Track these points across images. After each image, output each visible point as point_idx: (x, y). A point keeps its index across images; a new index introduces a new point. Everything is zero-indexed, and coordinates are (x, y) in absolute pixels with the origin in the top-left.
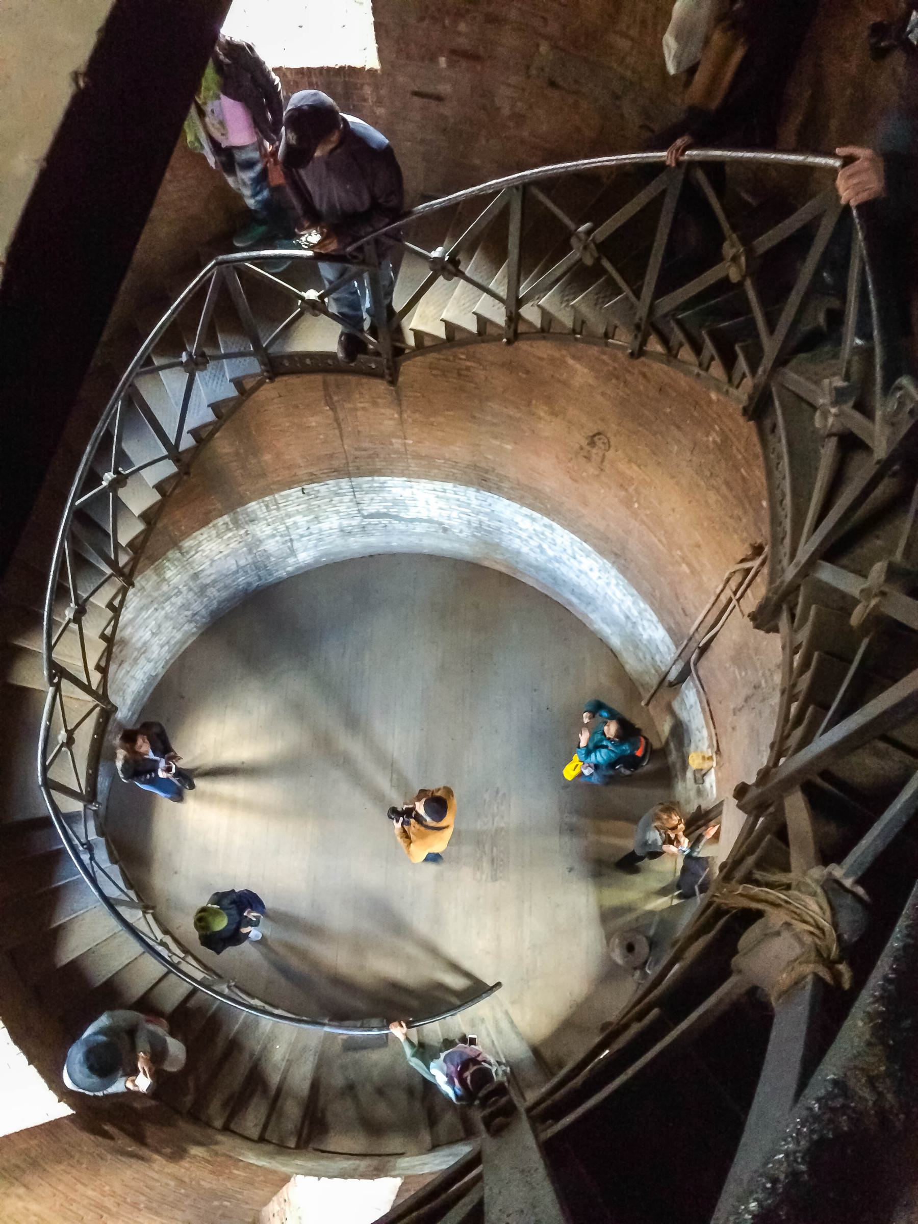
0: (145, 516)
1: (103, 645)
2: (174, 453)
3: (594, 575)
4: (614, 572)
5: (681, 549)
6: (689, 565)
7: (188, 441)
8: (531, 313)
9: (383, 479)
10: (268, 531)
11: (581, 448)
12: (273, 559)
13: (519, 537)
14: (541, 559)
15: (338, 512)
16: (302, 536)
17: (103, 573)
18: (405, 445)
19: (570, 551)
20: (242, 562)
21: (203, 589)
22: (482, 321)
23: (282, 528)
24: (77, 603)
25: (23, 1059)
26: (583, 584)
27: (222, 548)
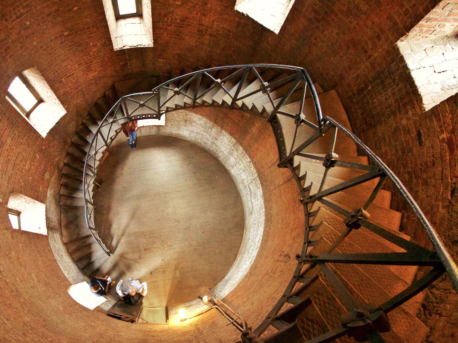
0: (214, 101)
2: (235, 99)
7: (239, 103)
11: (284, 252)
14: (248, 247)
15: (247, 177)
19: (251, 256)
20: (225, 152)
21: (213, 143)
23: (238, 161)
27: (226, 144)
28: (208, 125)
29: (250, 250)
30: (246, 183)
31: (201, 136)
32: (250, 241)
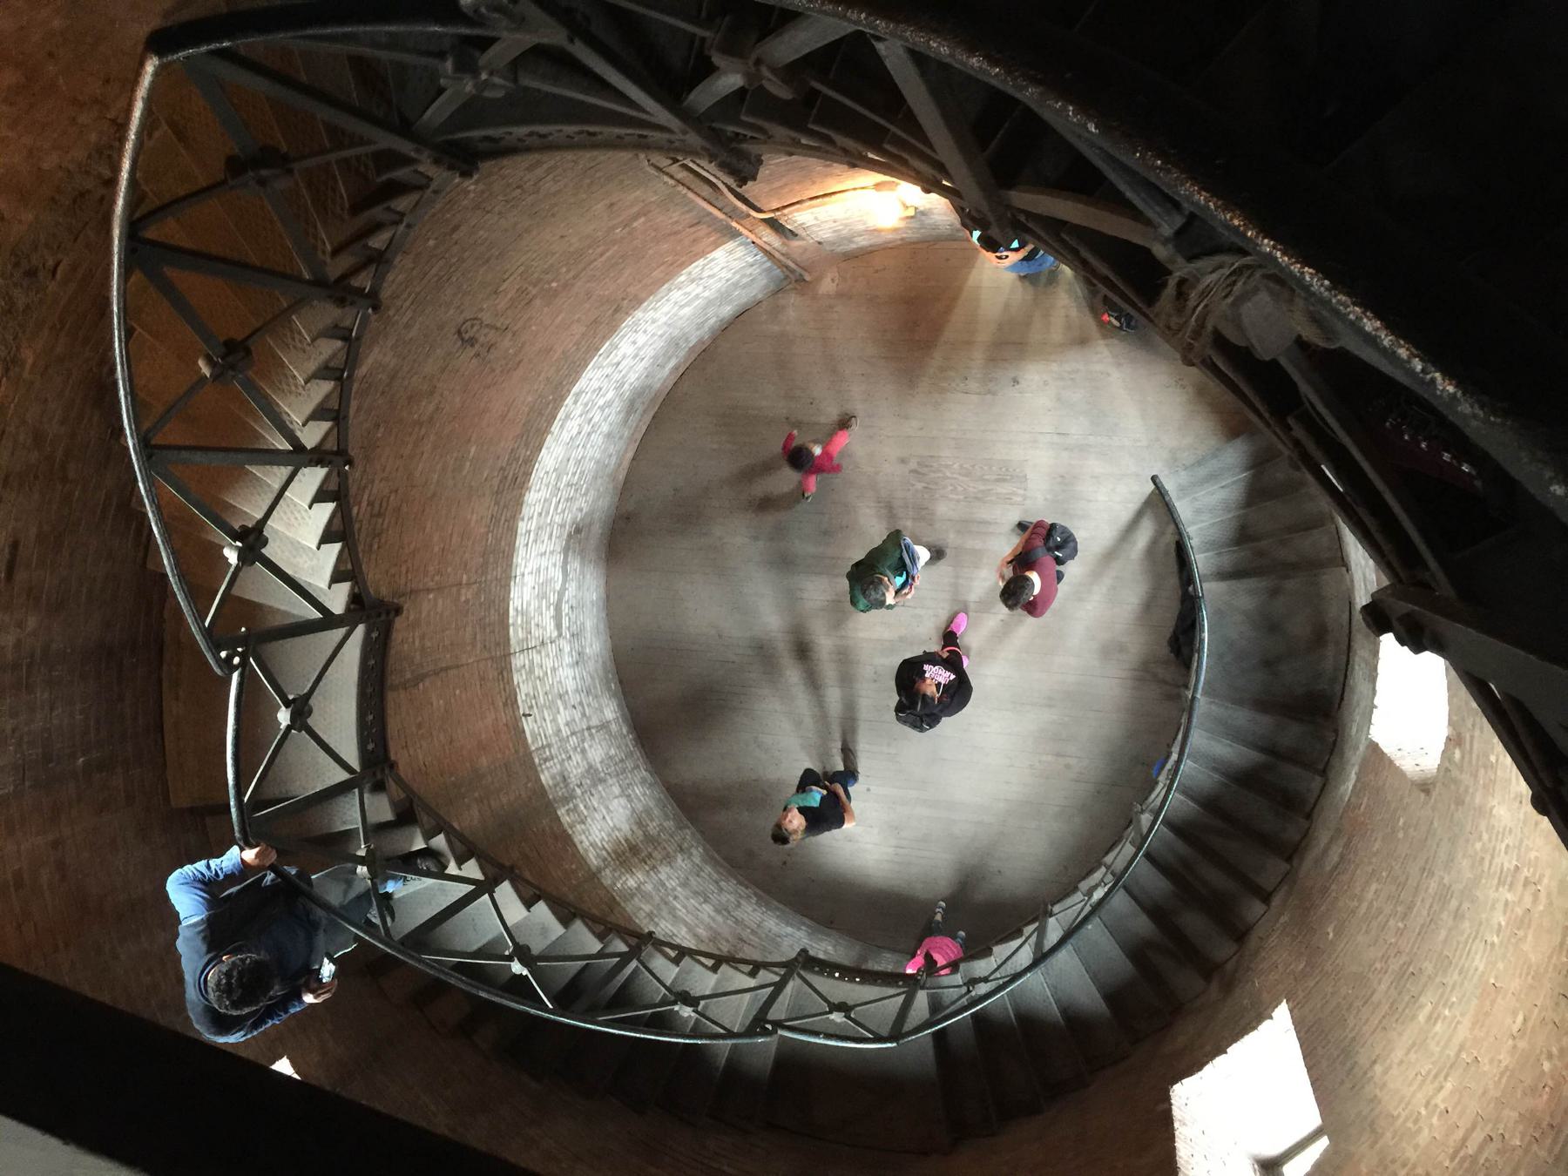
0: (566, 921)
1: (724, 968)
2: (485, 887)
3: (641, 339)
4: (639, 314)
5: (614, 228)
6: (636, 217)
7: (472, 869)
8: (311, 436)
9: (512, 612)
10: (577, 758)
12: (613, 752)
13: (589, 434)
14: (617, 406)
15: (554, 669)
16: (584, 714)
17: (636, 970)
18: (469, 584)
19: (609, 370)
20: (616, 790)
22: (320, 497)
23: (573, 740)
24: (675, 1003)
25: (1220, 1060)
26: (652, 353)
28: (647, 908)
29: (610, 395)
30: (567, 649)
31: (693, 881)
32: (605, 428)
